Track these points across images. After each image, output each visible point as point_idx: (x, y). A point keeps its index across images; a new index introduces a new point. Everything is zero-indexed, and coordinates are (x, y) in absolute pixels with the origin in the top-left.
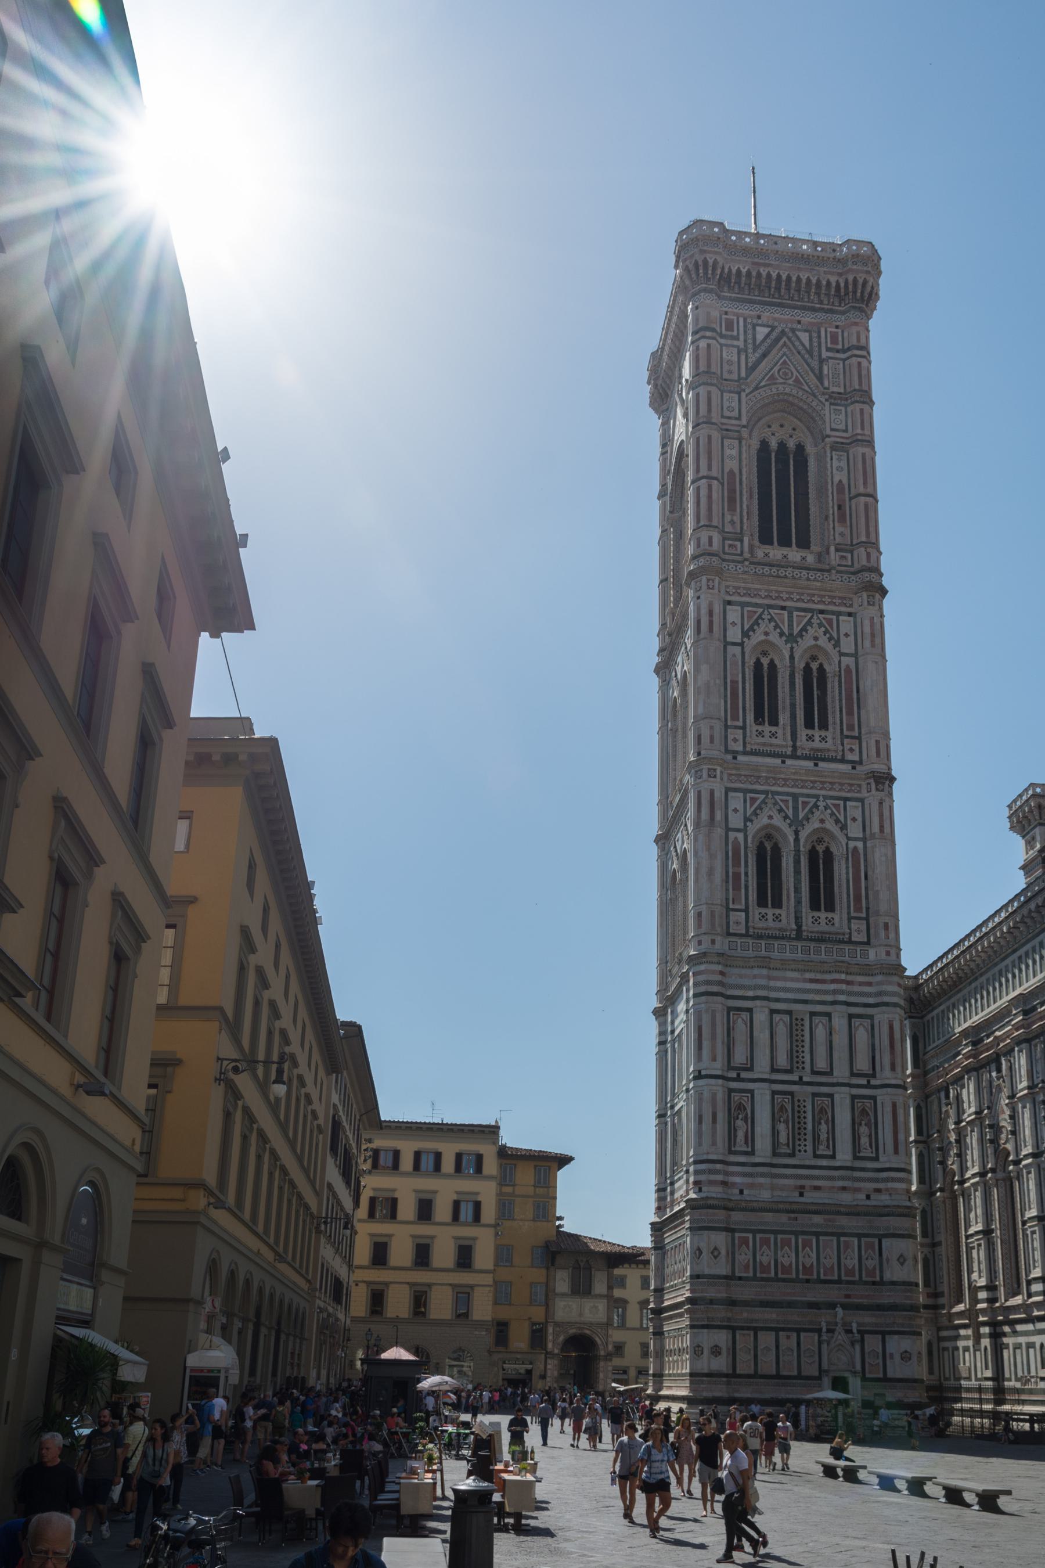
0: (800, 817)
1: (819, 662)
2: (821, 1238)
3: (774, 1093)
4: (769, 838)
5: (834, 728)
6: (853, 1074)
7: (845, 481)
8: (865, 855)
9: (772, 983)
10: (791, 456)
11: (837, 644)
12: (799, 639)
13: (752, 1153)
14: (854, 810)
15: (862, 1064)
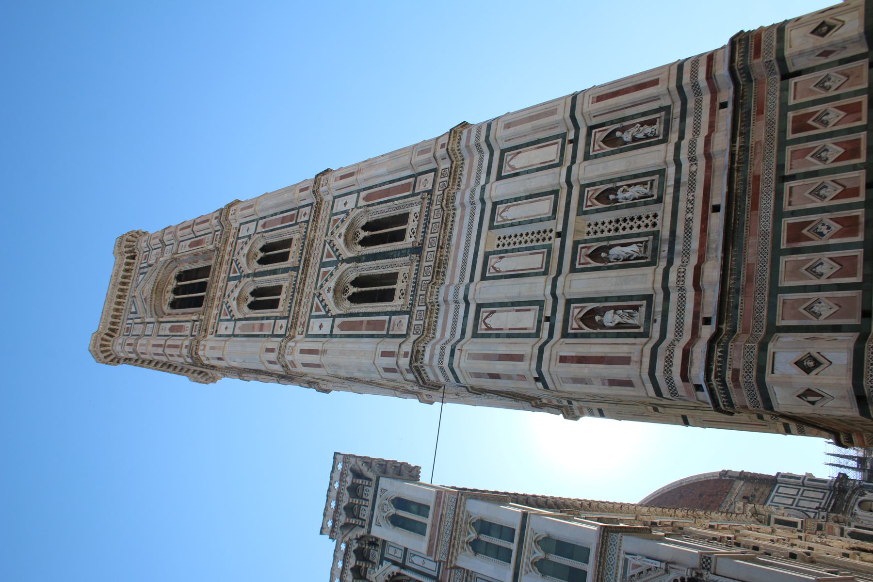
0: (336, 259)
1: (259, 252)
2: (788, 172)
3: (573, 270)
4: (346, 291)
5: (289, 233)
6: (560, 164)
7: (189, 242)
8: (369, 188)
9: (456, 281)
10: (180, 284)
11: (249, 237)
12: (241, 271)
13: (649, 298)
14: (339, 206)
15: (550, 153)
